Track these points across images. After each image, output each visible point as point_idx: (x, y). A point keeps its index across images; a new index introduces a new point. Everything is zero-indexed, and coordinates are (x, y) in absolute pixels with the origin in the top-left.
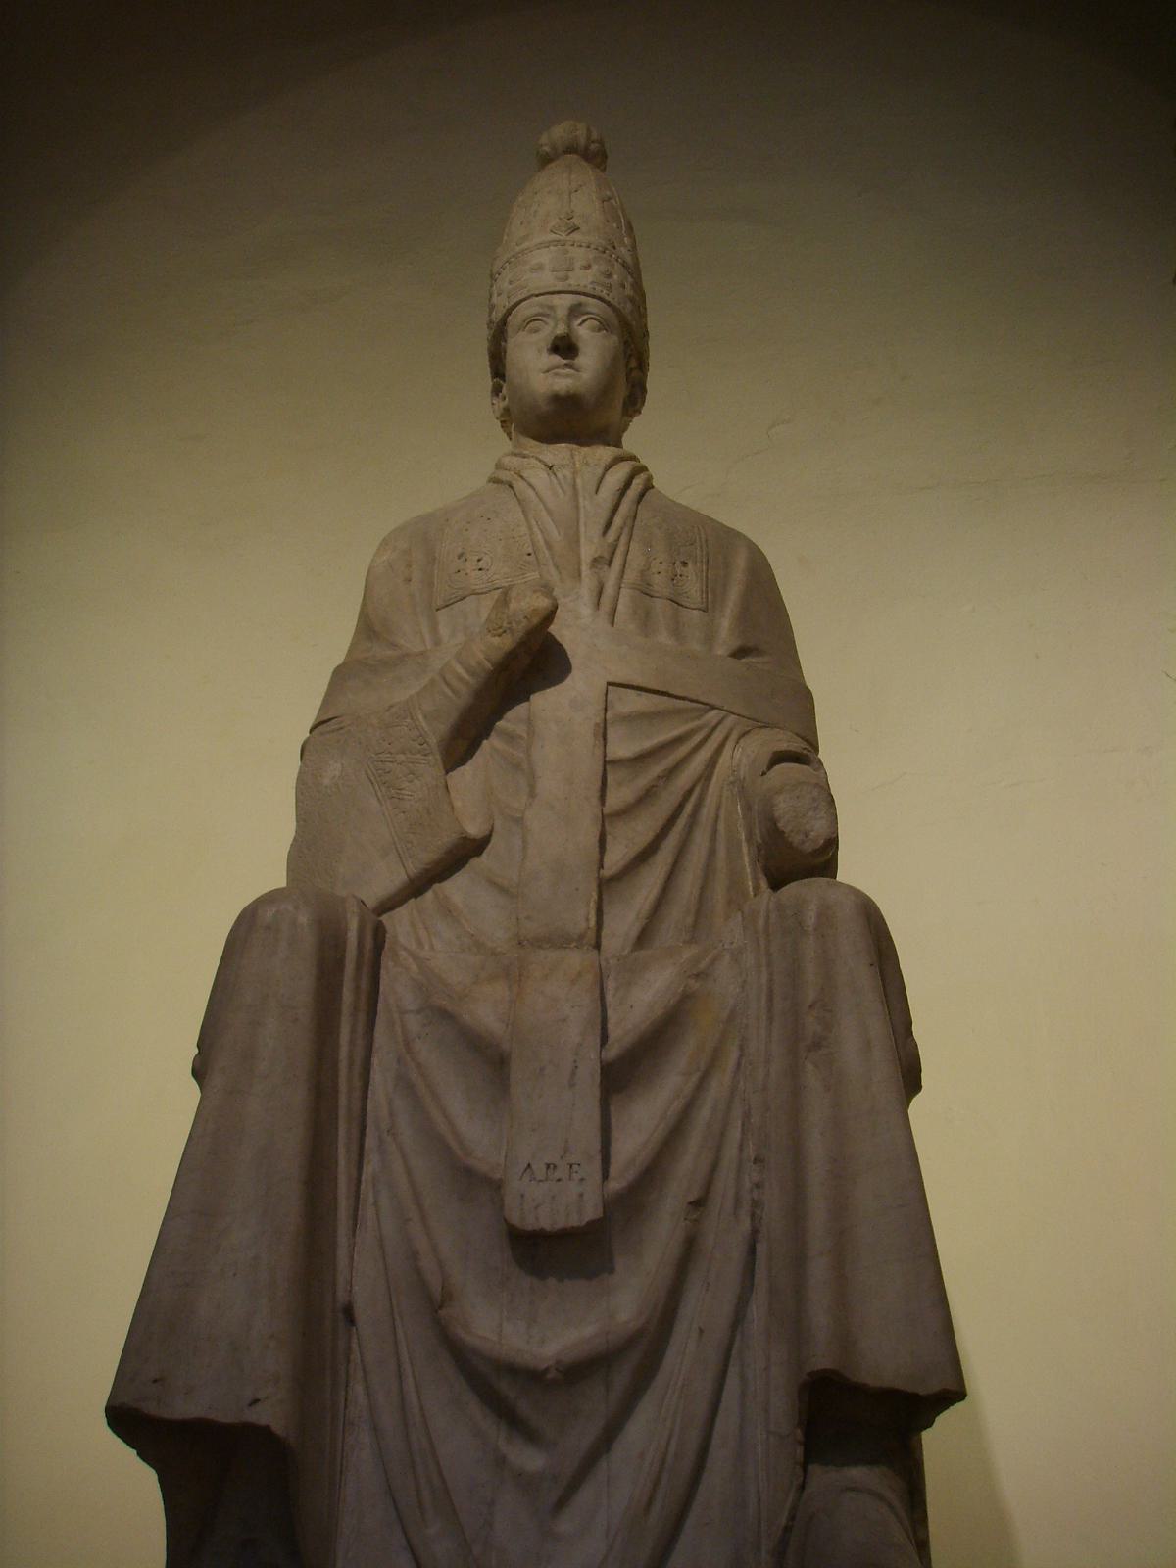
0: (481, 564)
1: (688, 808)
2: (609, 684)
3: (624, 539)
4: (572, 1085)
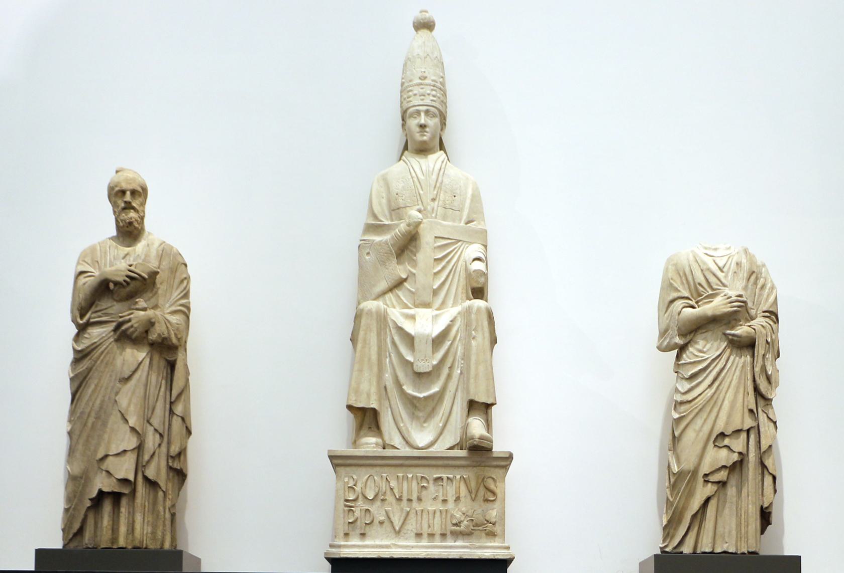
0: (403, 198)
1: (454, 270)
2: (436, 237)
3: (439, 190)
4: (426, 343)
